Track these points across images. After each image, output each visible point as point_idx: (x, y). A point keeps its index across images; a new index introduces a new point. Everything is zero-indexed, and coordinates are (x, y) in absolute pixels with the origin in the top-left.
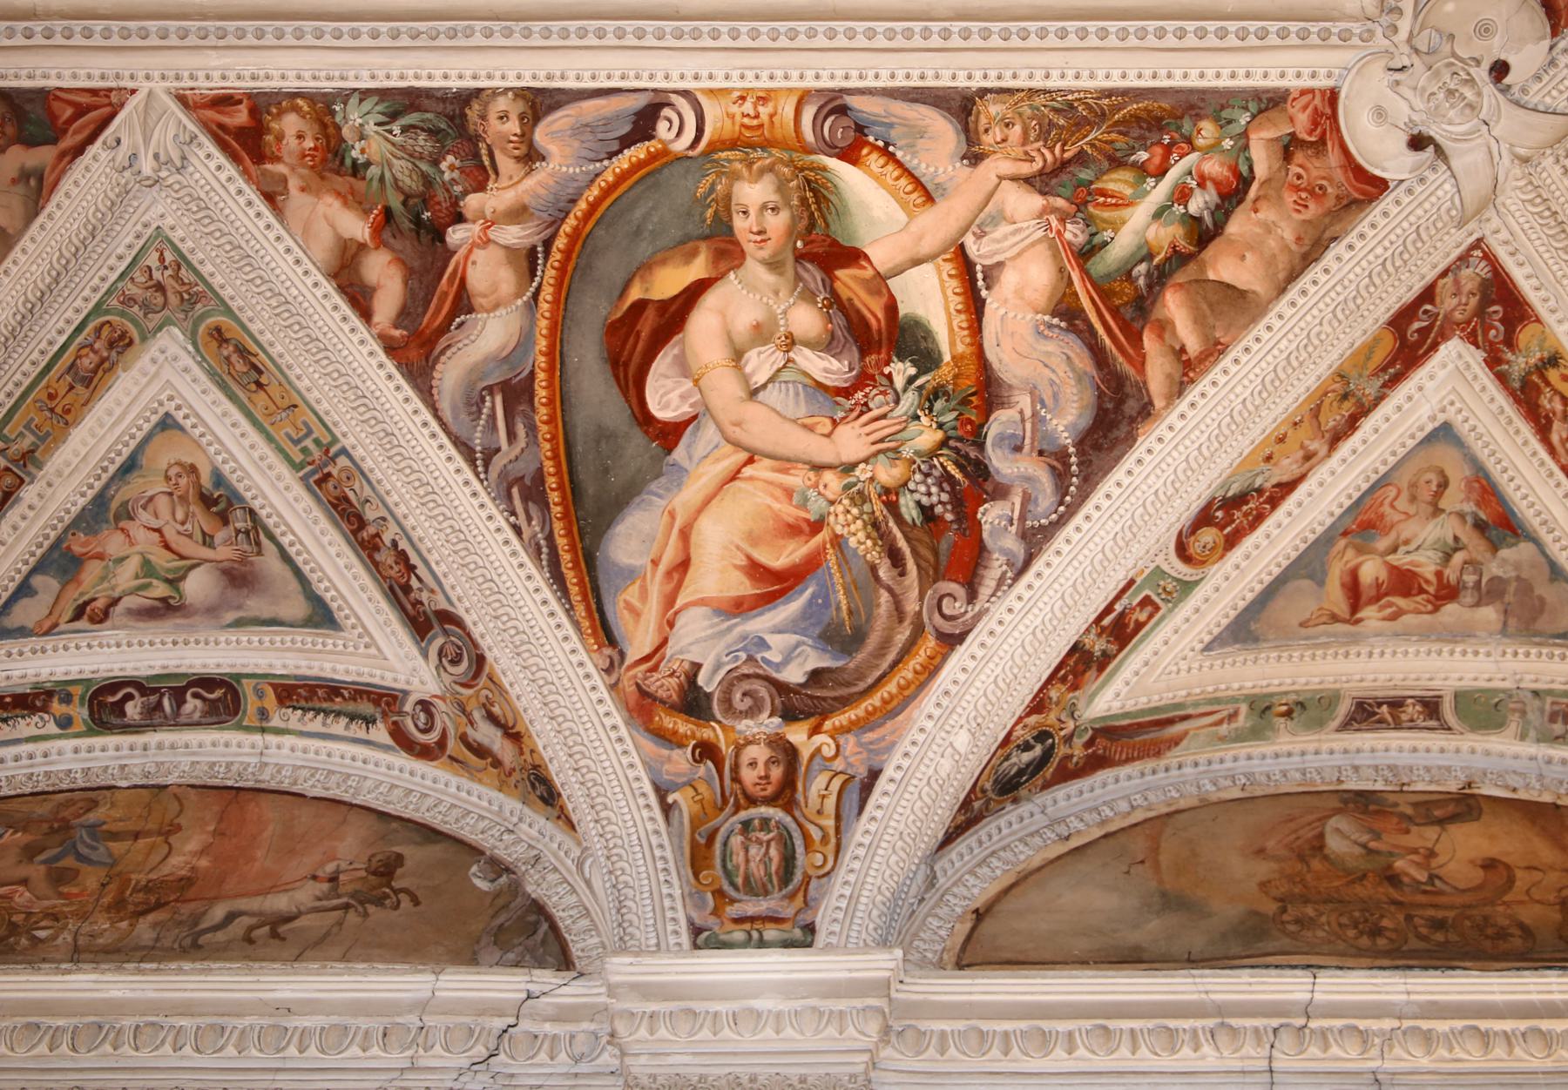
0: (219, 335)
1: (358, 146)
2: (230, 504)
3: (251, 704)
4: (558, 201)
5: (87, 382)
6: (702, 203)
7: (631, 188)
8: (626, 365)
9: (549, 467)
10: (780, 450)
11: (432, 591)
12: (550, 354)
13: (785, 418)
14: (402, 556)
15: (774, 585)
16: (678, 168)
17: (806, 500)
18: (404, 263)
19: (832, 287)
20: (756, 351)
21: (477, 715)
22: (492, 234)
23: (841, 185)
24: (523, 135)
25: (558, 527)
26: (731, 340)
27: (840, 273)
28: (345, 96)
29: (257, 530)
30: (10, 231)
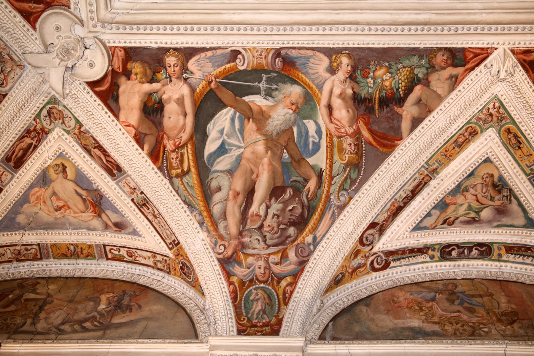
0: (508, 131)
2: (503, 187)
3: (496, 252)
30: (442, 96)
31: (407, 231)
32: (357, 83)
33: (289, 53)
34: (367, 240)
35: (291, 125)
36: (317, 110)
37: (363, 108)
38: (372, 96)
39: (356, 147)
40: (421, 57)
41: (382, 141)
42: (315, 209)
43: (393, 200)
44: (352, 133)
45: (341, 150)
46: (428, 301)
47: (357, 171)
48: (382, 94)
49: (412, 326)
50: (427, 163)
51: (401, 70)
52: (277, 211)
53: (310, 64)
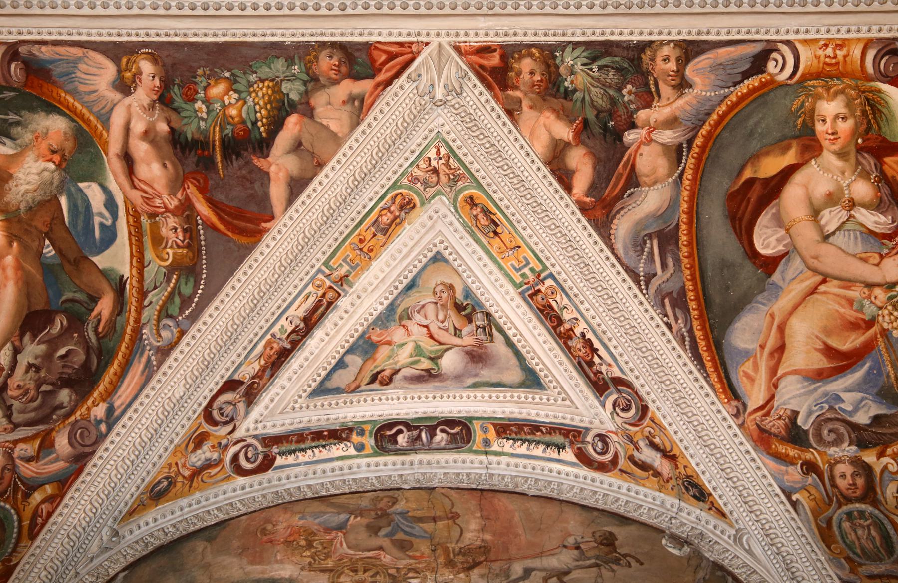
0: (472, 202)
1: (569, 79)
2: (474, 309)
3: (479, 436)
4: (699, 114)
5: (385, 232)
6: (795, 115)
7: (748, 105)
8: (741, 220)
9: (689, 286)
10: (844, 275)
11: (610, 365)
12: (690, 213)
13: (847, 254)
14: (589, 343)
15: (841, 361)
16: (780, 92)
17: (862, 306)
18: (594, 155)
19: (881, 169)
20: (828, 210)
21: (641, 444)
22: (654, 136)
23: (890, 101)
24: (678, 71)
25: (696, 324)
26: (811, 203)
27: (887, 160)
28: (563, 46)
29: (491, 325)
30: (340, 135)
31: (300, 397)
32: (176, 110)
33: (37, 54)
34: (222, 415)
35: (55, 192)
36: (102, 163)
37: (192, 159)
38: (206, 137)
39: (188, 235)
40: (290, 61)
41: (236, 222)
42: (111, 355)
43: (269, 336)
44: (176, 207)
45: (158, 241)
46: (328, 530)
47: (192, 280)
48: (226, 132)
49: (277, 577)
50: (326, 264)
51: (256, 86)
52: (36, 358)
53: (79, 74)
